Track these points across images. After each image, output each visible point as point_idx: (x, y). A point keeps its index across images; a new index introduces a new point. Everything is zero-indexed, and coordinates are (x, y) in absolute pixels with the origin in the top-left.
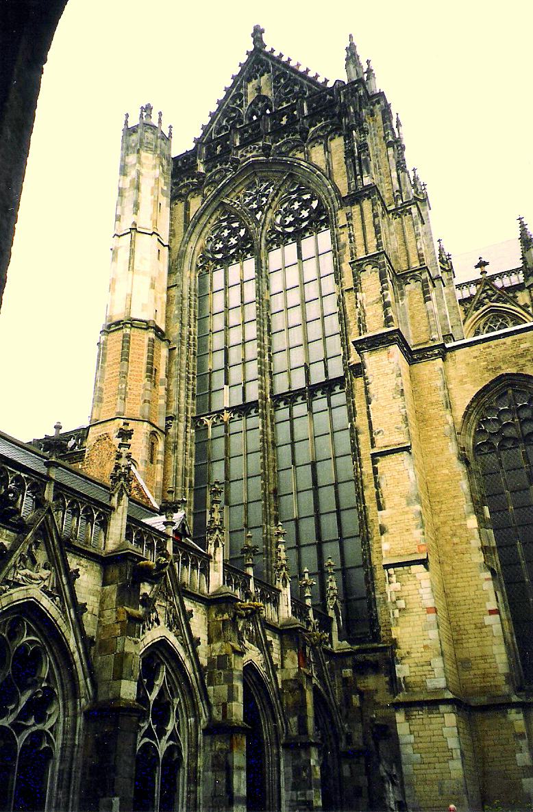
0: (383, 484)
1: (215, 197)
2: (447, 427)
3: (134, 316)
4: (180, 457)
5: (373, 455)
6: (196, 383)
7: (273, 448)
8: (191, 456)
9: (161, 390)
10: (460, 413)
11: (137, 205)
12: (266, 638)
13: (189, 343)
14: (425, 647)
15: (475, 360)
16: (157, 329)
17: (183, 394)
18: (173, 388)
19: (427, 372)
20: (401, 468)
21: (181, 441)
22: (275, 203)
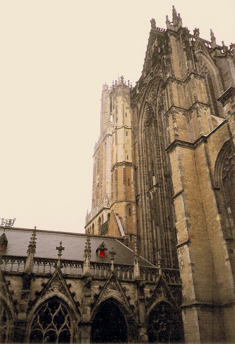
0: (176, 210)
1: (143, 101)
2: (207, 174)
3: (118, 162)
4: (144, 210)
5: (173, 198)
6: (147, 178)
7: (167, 199)
8: (148, 208)
9: (133, 186)
10: (213, 166)
11: (117, 119)
12: (121, 287)
13: (143, 163)
14: (189, 281)
15: (216, 138)
16: (127, 164)
17: (143, 184)
18: (139, 183)
19: (200, 151)
20: (180, 202)
21: (144, 203)
22: (159, 94)
